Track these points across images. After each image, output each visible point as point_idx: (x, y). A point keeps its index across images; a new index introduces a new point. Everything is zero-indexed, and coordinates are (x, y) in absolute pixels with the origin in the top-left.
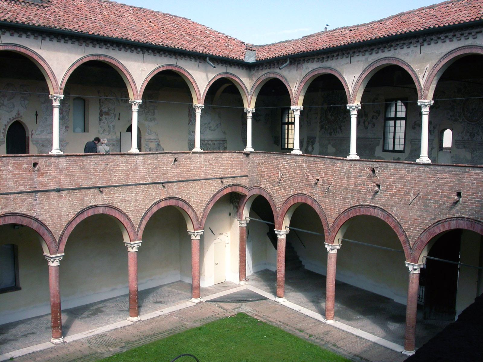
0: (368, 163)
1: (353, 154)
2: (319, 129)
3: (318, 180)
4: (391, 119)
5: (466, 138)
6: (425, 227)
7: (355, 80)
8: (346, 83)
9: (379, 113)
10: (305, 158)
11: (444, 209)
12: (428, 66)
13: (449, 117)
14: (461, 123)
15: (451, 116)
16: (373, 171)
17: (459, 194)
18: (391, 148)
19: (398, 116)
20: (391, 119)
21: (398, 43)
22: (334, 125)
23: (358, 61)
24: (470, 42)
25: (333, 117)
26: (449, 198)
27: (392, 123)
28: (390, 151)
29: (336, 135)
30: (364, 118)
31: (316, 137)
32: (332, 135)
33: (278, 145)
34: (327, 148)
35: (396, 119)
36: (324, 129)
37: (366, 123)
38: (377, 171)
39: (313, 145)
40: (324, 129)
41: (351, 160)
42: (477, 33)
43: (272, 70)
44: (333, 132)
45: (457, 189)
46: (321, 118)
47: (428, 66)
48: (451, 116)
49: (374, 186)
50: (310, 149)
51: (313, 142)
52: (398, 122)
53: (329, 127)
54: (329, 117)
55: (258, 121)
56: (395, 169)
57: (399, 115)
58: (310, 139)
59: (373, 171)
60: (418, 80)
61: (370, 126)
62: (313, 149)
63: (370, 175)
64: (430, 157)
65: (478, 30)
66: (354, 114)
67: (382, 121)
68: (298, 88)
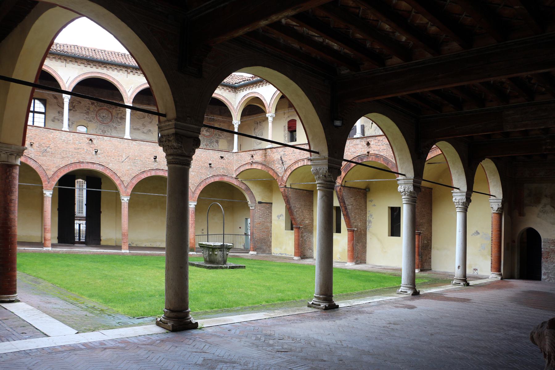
6: (134, 175)
56: (110, 141)
63: (89, 143)
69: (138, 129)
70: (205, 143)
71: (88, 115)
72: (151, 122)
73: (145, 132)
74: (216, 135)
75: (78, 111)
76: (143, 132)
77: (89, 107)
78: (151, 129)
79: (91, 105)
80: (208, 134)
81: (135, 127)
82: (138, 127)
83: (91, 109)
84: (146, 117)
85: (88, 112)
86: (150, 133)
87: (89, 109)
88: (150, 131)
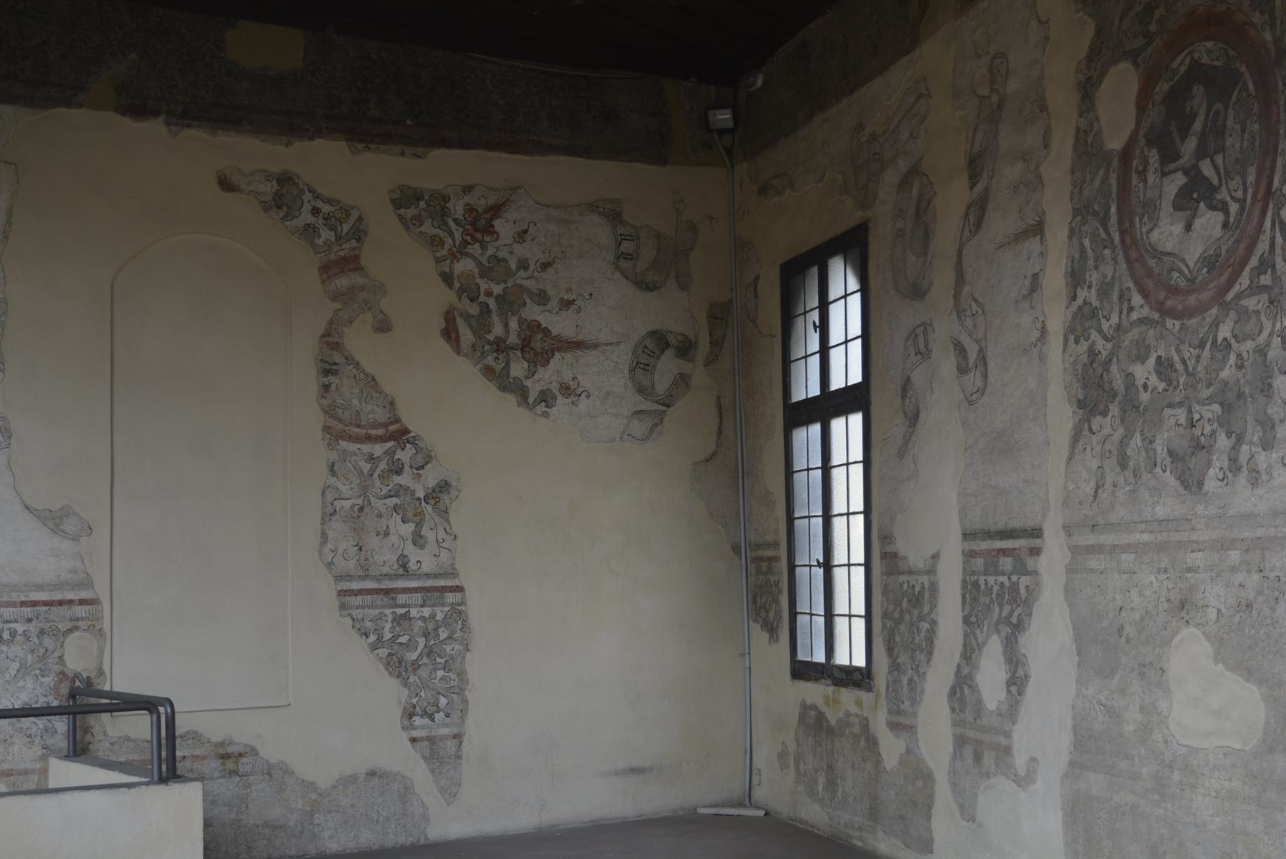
2: (1062, 416)
22: (1224, 332)
25: (1209, 222)
29: (1254, 483)
31: (1036, 533)
32: (1211, 484)
34: (1153, 674)
36: (1114, 409)
39: (1018, 627)
40: (1114, 409)
44: (1223, 442)
46: (1076, 278)
51: (1014, 588)
53: (1164, 368)
55: (546, 398)
58: (992, 568)
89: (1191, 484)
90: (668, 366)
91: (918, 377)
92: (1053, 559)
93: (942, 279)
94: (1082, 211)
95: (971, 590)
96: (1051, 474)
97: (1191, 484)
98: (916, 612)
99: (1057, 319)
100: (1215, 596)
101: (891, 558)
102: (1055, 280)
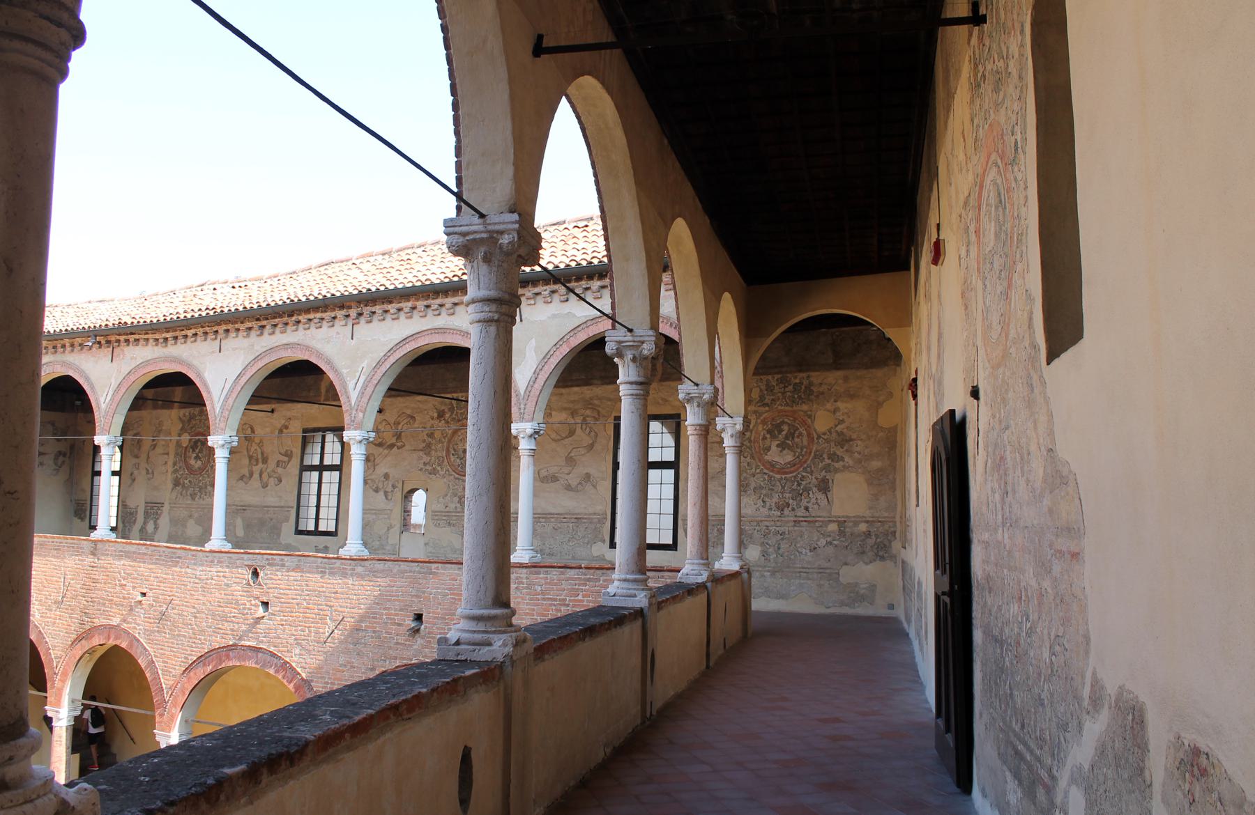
0: (246, 556)
1: (217, 540)
2: (170, 486)
3: (144, 594)
4: (312, 468)
5: (452, 506)
7: (228, 387)
8: (209, 392)
9: (289, 455)
10: (120, 547)
11: (390, 648)
12: (364, 364)
13: (421, 466)
14: (444, 477)
15: (425, 464)
16: (255, 574)
17: (419, 617)
18: (311, 527)
19: (326, 463)
20: (312, 468)
21: (311, 316)
23: (234, 349)
24: (443, 321)
26: (399, 625)
27: (315, 474)
28: (309, 533)
30: (260, 465)
33: (82, 519)
35: (321, 468)
37: (265, 475)
38: (261, 574)
41: (211, 551)
42: (455, 304)
43: (59, 357)
45: (416, 608)
46: (175, 464)
47: (364, 364)
48: (425, 464)
49: (256, 606)
50: (150, 527)
52: (326, 474)
54: (192, 462)
57: (327, 462)
58: (152, 508)
59: (255, 574)
60: (346, 392)
61: (272, 481)
62: (156, 528)
64: (365, 544)
65: (456, 300)
66: (221, 456)
67: (297, 472)
68: (113, 399)
69: (554, 479)
70: (776, 498)
71: (428, 454)
72: (591, 447)
73: (574, 483)
74: (818, 456)
75: (407, 447)
76: (568, 488)
77: (432, 426)
78: (592, 471)
79: (437, 422)
80: (788, 457)
81: (544, 473)
82: (554, 470)
83: (438, 435)
84: (578, 431)
85: (429, 446)
86: (588, 487)
87: (431, 435)
88: (588, 477)
89: (193, 499)
90: (61, 459)
91: (136, 472)
92: (166, 508)
93: (144, 456)
94: (177, 454)
95: (146, 513)
96: (166, 494)
97: (193, 499)
98: (196, 515)
99: (171, 470)
100: (196, 515)
101: (125, 506)
102: (170, 463)
